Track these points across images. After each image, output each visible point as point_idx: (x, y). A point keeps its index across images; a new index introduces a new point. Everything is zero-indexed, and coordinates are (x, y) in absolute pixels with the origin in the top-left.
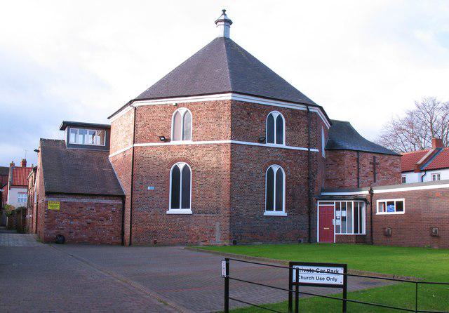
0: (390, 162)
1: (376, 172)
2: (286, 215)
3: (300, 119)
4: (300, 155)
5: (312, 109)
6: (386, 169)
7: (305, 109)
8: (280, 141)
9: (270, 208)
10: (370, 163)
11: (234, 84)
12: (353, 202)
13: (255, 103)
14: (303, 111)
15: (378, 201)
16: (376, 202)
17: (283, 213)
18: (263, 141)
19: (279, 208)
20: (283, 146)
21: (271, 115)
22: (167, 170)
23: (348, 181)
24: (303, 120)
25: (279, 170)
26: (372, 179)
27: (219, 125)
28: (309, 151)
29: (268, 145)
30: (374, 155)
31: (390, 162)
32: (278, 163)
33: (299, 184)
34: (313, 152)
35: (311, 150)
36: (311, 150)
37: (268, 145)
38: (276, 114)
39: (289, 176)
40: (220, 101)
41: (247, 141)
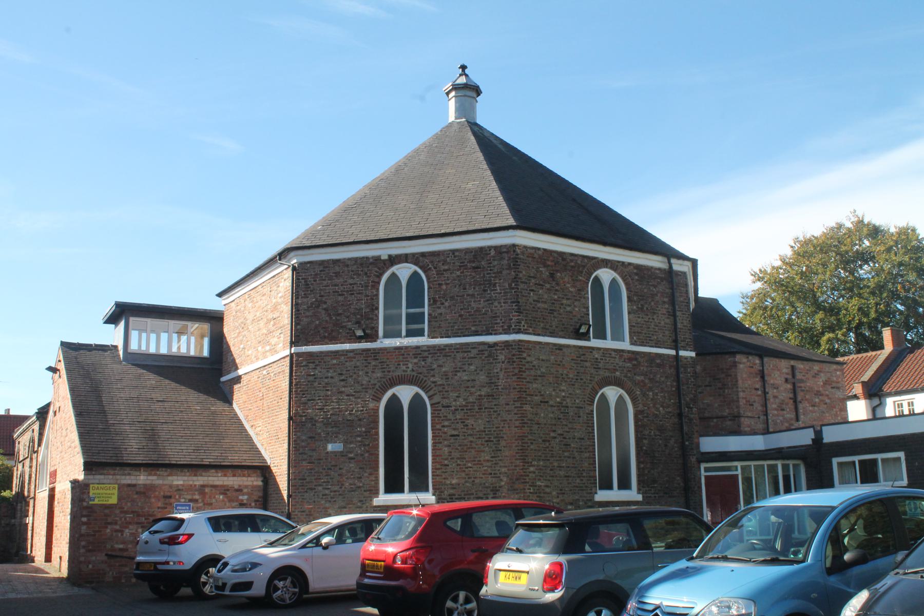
0: (823, 377)
1: (799, 398)
2: (639, 498)
3: (655, 286)
4: (659, 366)
5: (677, 266)
6: (818, 394)
7: (664, 266)
8: (617, 337)
9: (607, 485)
10: (786, 380)
11: (515, 210)
12: (779, 464)
13: (564, 253)
14: (659, 269)
15: (835, 461)
16: (831, 463)
17: (633, 494)
18: (585, 336)
19: (624, 484)
20: (625, 345)
21: (597, 280)
22: (437, 399)
23: (745, 422)
24: (661, 288)
25: (621, 399)
26: (793, 416)
27: (490, 300)
28: (677, 356)
29: (594, 343)
30: (792, 363)
31: (823, 377)
32: (618, 383)
33: (661, 429)
34: (686, 358)
35: (673, 352)
36: (673, 352)
37: (594, 343)
38: (606, 275)
39: (641, 412)
40: (490, 248)
41: (552, 334)
